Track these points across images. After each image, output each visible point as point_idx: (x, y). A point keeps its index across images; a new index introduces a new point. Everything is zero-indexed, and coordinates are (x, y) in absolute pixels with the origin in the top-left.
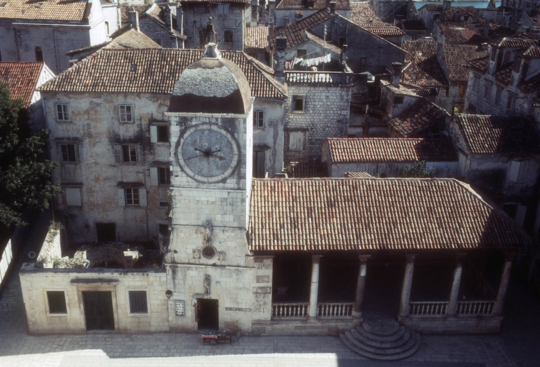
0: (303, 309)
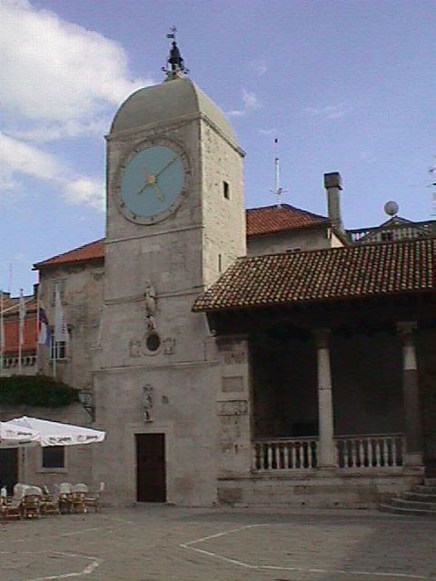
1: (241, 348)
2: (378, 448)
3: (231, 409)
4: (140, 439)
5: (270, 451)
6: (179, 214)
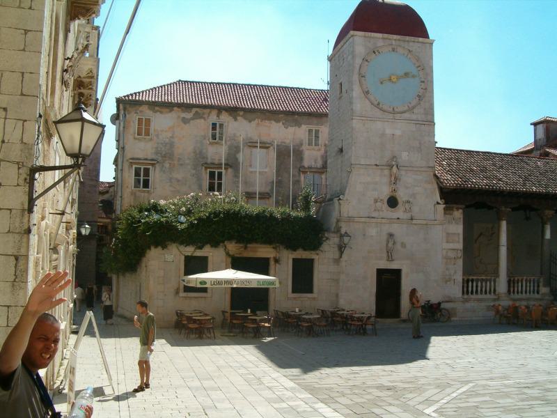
0: (492, 283)
1: (458, 214)
2: (528, 284)
3: (451, 254)
4: (380, 272)
5: (470, 284)
6: (415, 111)
